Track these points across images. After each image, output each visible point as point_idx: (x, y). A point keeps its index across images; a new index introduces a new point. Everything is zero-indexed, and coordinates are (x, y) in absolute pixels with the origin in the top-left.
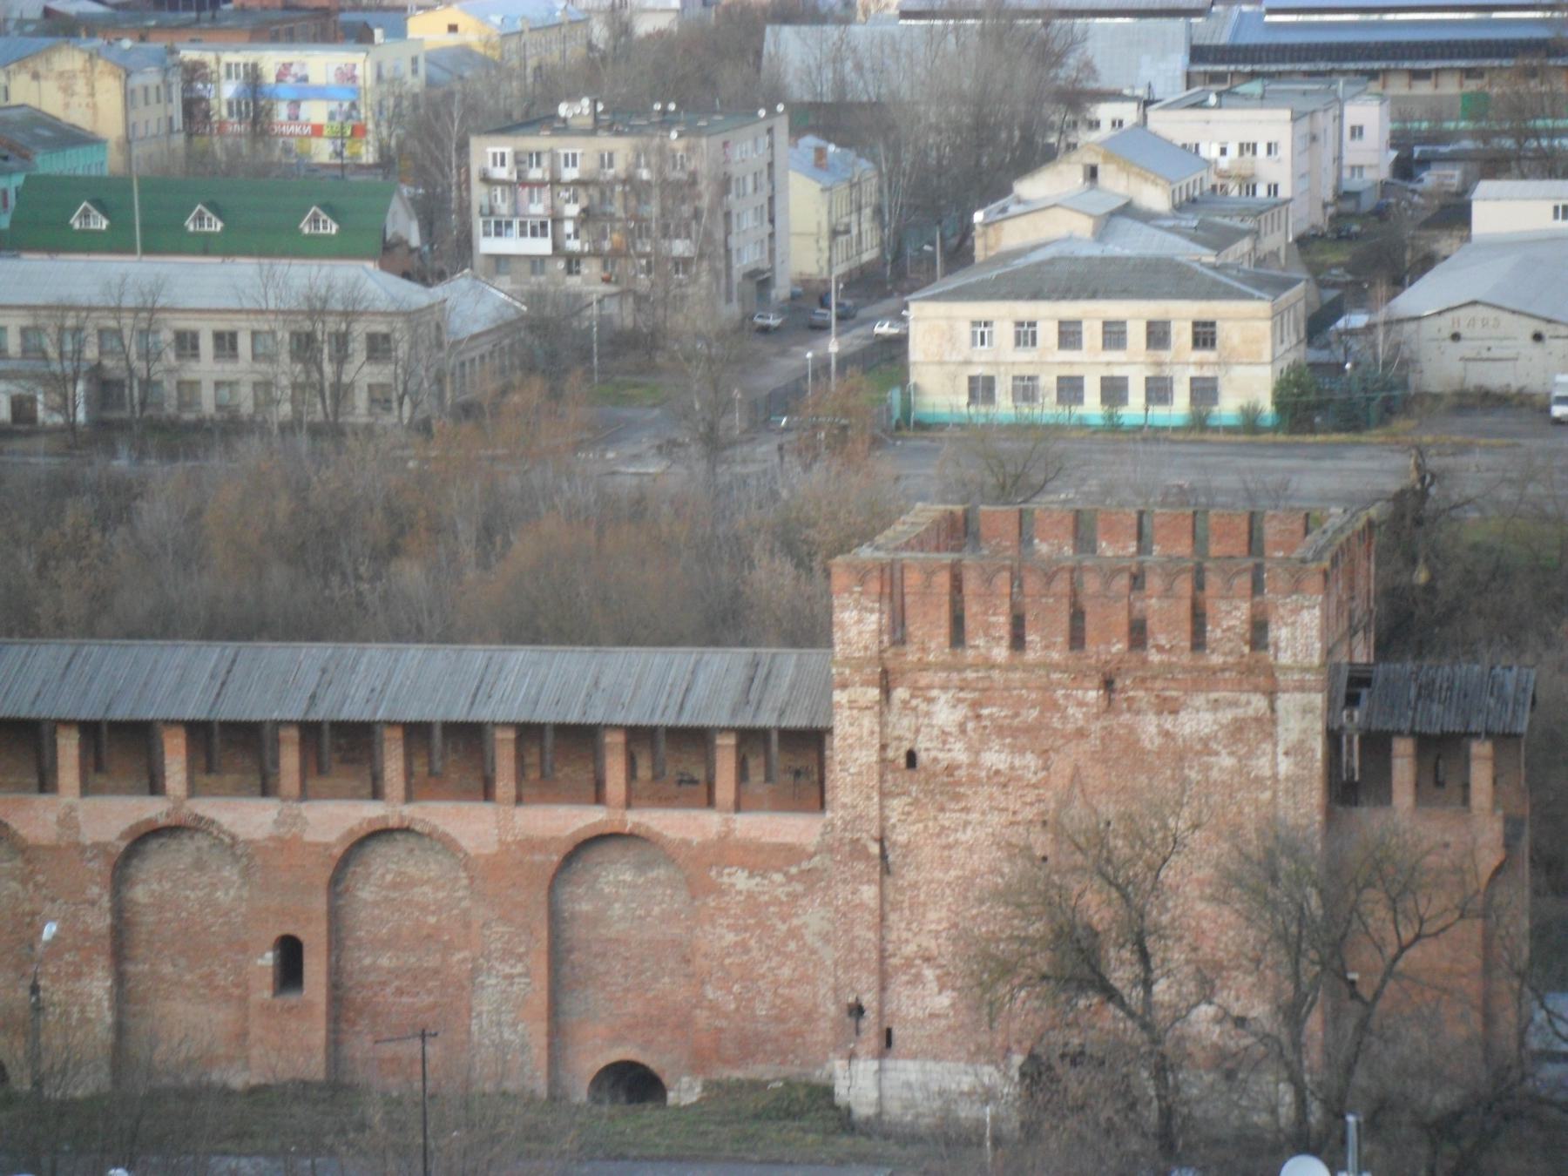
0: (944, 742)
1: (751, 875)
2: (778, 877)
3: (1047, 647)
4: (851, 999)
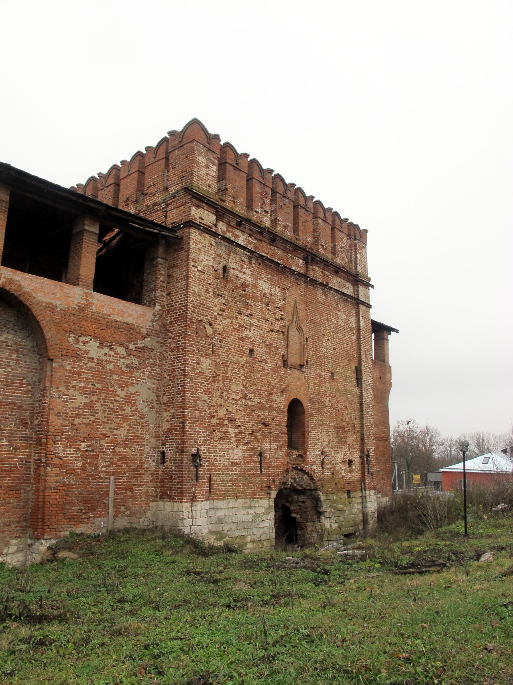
1: (101, 346)
2: (121, 350)
4: (194, 451)
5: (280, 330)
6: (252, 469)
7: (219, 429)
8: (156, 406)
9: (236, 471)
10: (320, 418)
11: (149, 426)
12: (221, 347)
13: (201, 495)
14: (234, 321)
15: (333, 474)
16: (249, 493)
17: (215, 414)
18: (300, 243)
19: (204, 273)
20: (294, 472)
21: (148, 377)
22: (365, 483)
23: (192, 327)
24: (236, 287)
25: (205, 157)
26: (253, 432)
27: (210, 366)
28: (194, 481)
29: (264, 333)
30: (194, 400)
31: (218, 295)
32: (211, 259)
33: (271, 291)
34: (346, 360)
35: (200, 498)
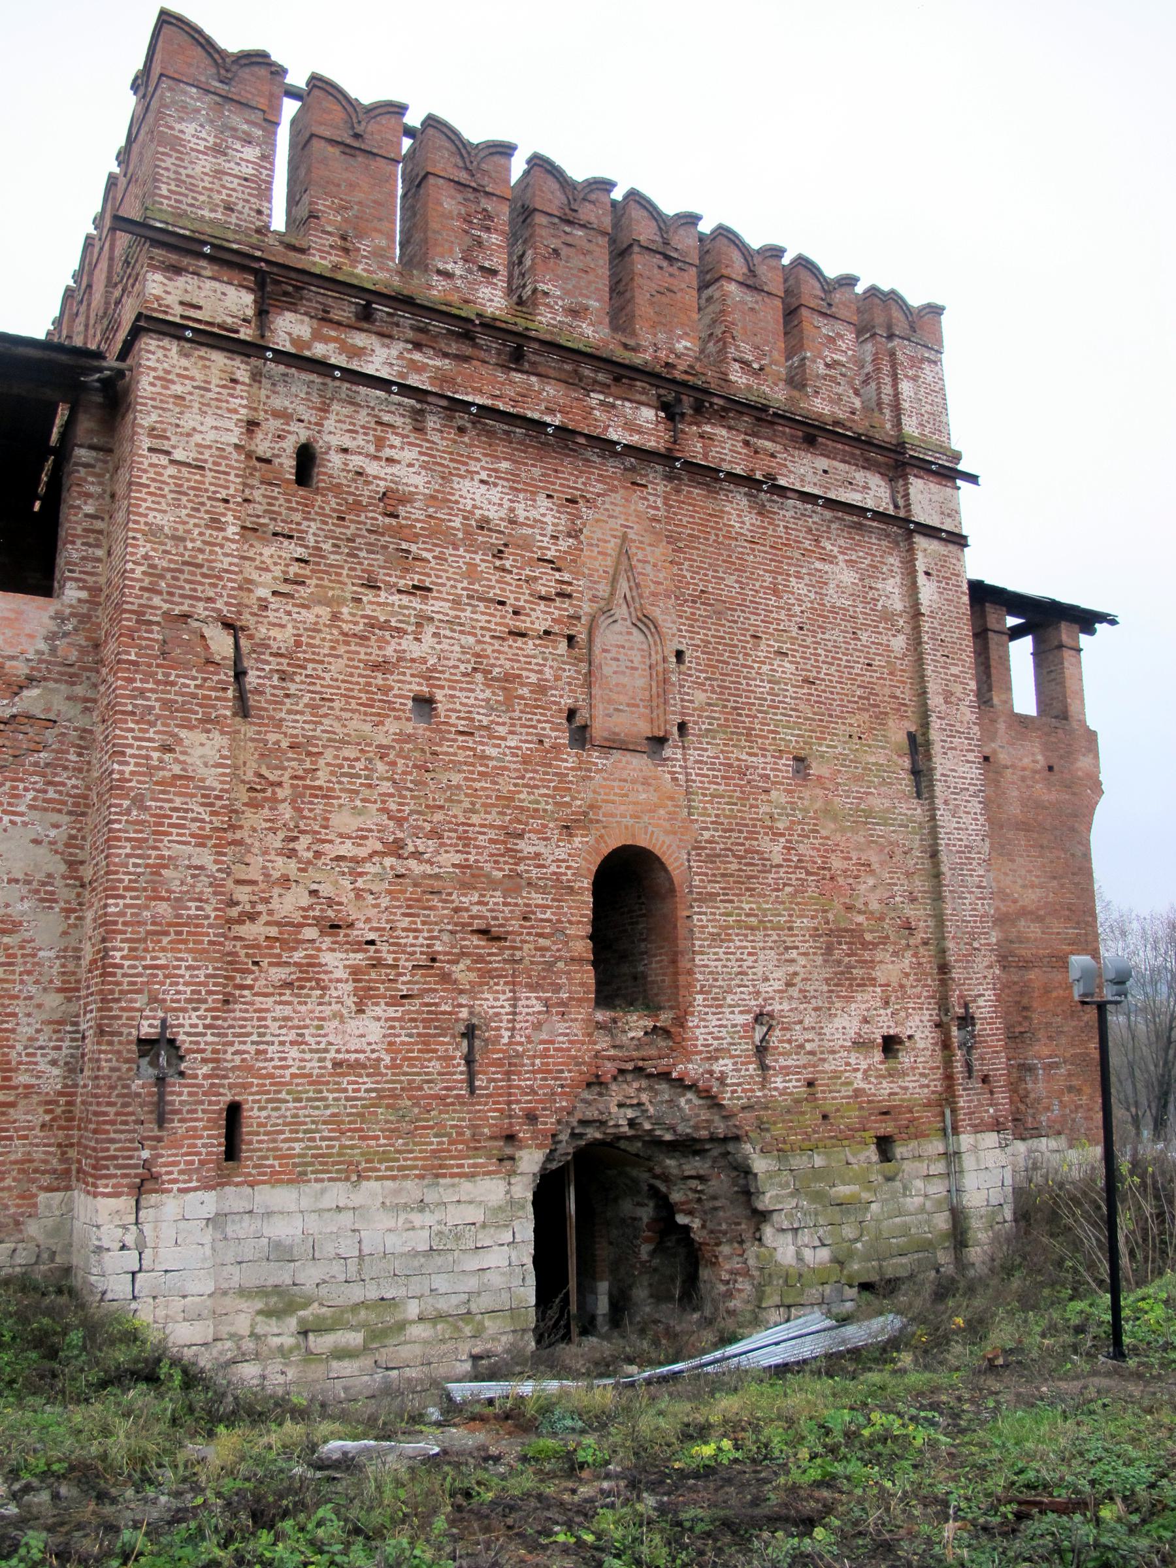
0: (380, 443)
3: (574, 312)
5: (556, 629)
6: (428, 1082)
7: (279, 956)
8: (65, 894)
9: (355, 1091)
10: (746, 907)
11: (34, 956)
12: (287, 696)
13: (181, 1172)
14: (345, 610)
15: (810, 1084)
16: (415, 1159)
17: (260, 908)
18: (638, 359)
19: (202, 468)
20: (636, 1085)
21: (31, 807)
22: (953, 1111)
23: (140, 638)
24: (357, 507)
25: (212, 122)
26: (433, 960)
27: (222, 757)
28: (151, 1129)
29: (479, 642)
30: (147, 866)
31: (275, 534)
32: (231, 425)
33: (512, 510)
34: (866, 715)
35: (175, 1181)
